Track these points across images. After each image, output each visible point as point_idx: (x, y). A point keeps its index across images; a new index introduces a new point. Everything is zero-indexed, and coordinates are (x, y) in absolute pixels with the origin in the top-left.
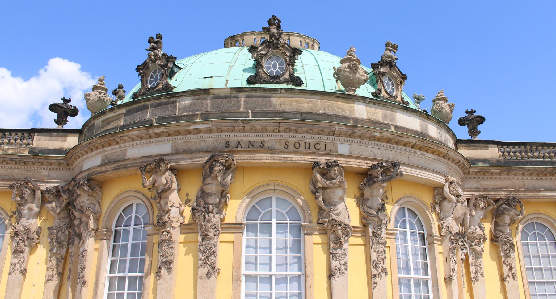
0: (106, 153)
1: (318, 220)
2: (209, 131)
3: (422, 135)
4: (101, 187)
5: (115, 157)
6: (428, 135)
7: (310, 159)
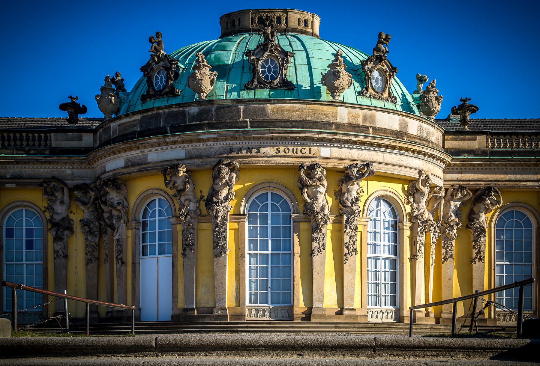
0: (128, 157)
1: (304, 211)
2: (216, 140)
3: (400, 135)
4: (125, 186)
5: (137, 161)
6: (406, 133)
7: (297, 161)
